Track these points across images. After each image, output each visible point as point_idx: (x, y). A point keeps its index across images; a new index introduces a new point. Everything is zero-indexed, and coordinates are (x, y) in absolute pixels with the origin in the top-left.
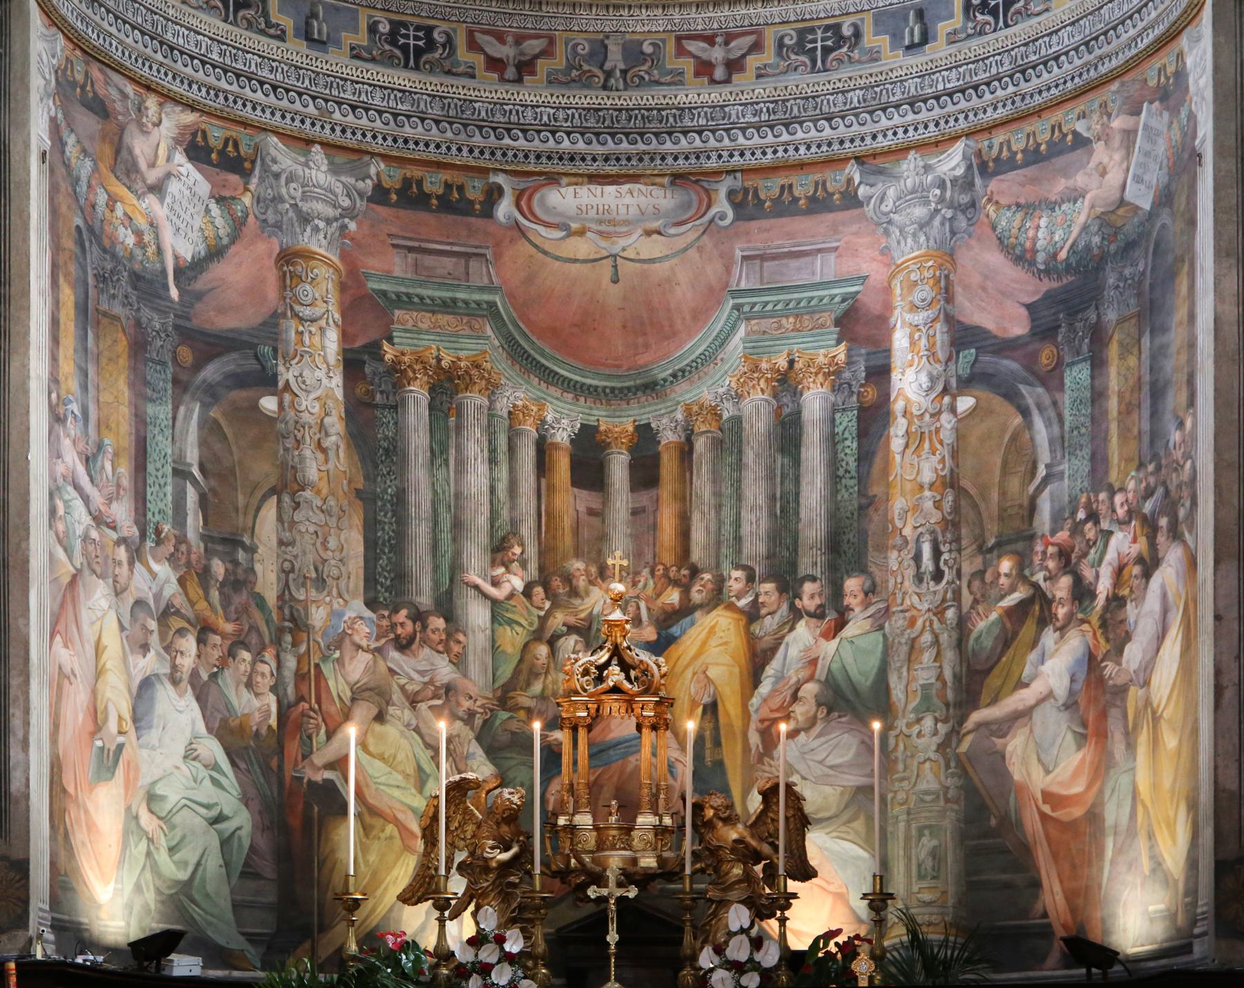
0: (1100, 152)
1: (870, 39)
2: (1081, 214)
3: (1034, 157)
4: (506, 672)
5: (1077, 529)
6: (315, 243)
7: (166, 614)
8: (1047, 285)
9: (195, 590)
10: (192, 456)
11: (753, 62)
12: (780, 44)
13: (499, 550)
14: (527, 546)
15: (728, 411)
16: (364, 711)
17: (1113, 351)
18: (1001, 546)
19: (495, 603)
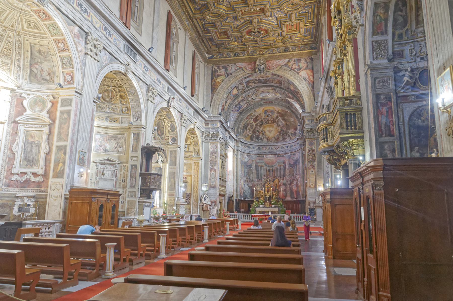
2: (296, 158)
13: (264, 176)
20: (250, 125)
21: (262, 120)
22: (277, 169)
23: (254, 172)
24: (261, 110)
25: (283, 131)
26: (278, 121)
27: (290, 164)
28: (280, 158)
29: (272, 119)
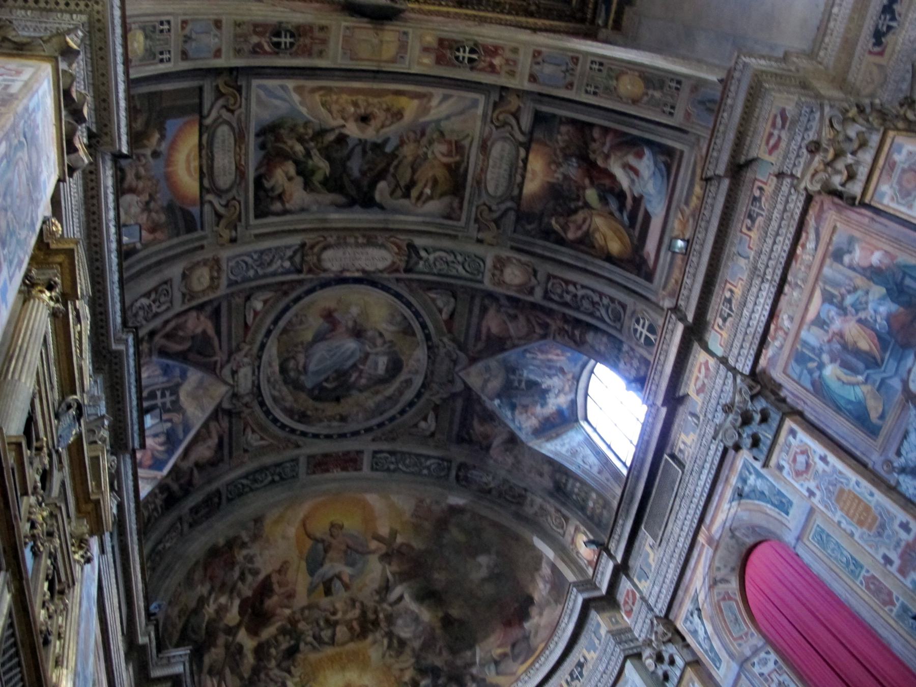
20: (221, 640)
21: (293, 621)
26: (390, 619)
29: (357, 612)
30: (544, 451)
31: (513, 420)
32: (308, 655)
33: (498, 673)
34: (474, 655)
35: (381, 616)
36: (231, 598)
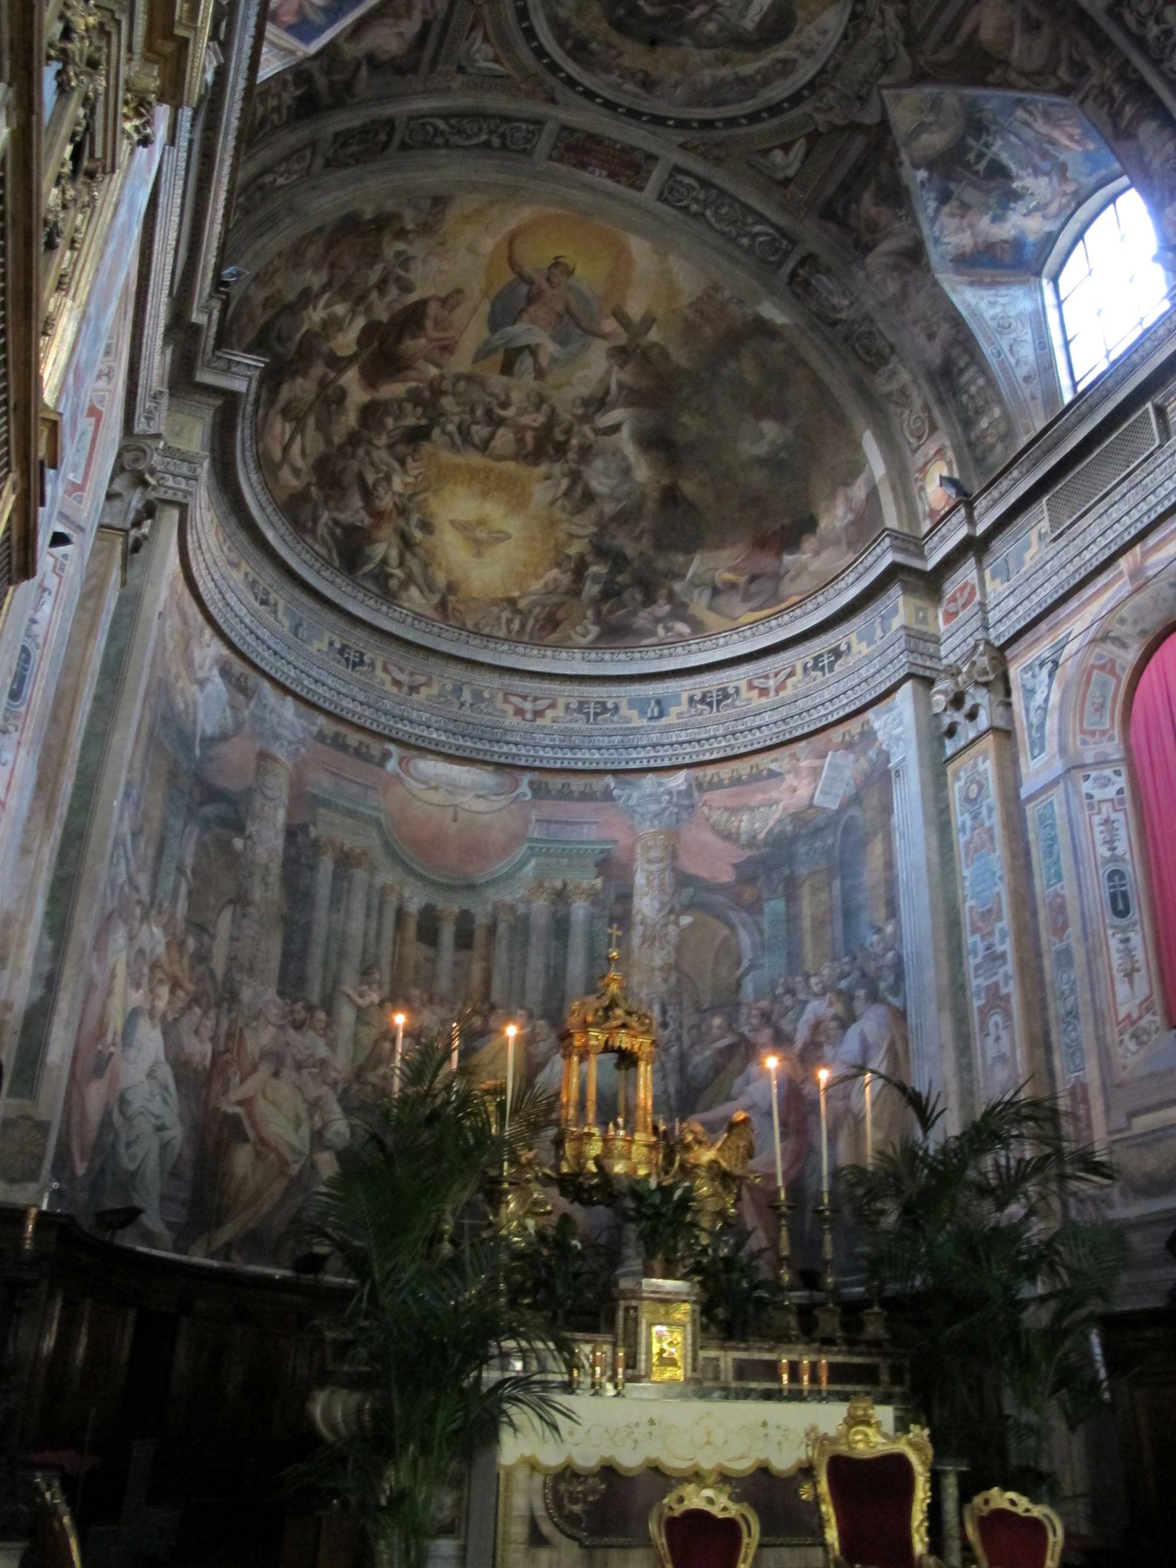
0: (790, 780)
1: (624, 710)
2: (777, 813)
3: (737, 781)
4: (361, 1059)
5: (776, 999)
6: (281, 754)
7: (155, 966)
8: (748, 853)
9: (175, 955)
10: (189, 862)
11: (550, 713)
12: (567, 707)
13: (366, 973)
14: (384, 973)
15: (521, 909)
16: (265, 1069)
17: (805, 891)
18: (714, 1009)
19: (359, 1009)
20: (318, 370)
21: (437, 391)
22: (521, 927)
23: (257, 894)
24: (488, 244)
25: (618, 561)
26: (586, 453)
27: (683, 880)
28: (553, 808)
29: (538, 419)
30: (955, 299)
31: (933, 220)
32: (439, 449)
33: (710, 607)
34: (688, 564)
35: (574, 442)
36: (353, 313)
